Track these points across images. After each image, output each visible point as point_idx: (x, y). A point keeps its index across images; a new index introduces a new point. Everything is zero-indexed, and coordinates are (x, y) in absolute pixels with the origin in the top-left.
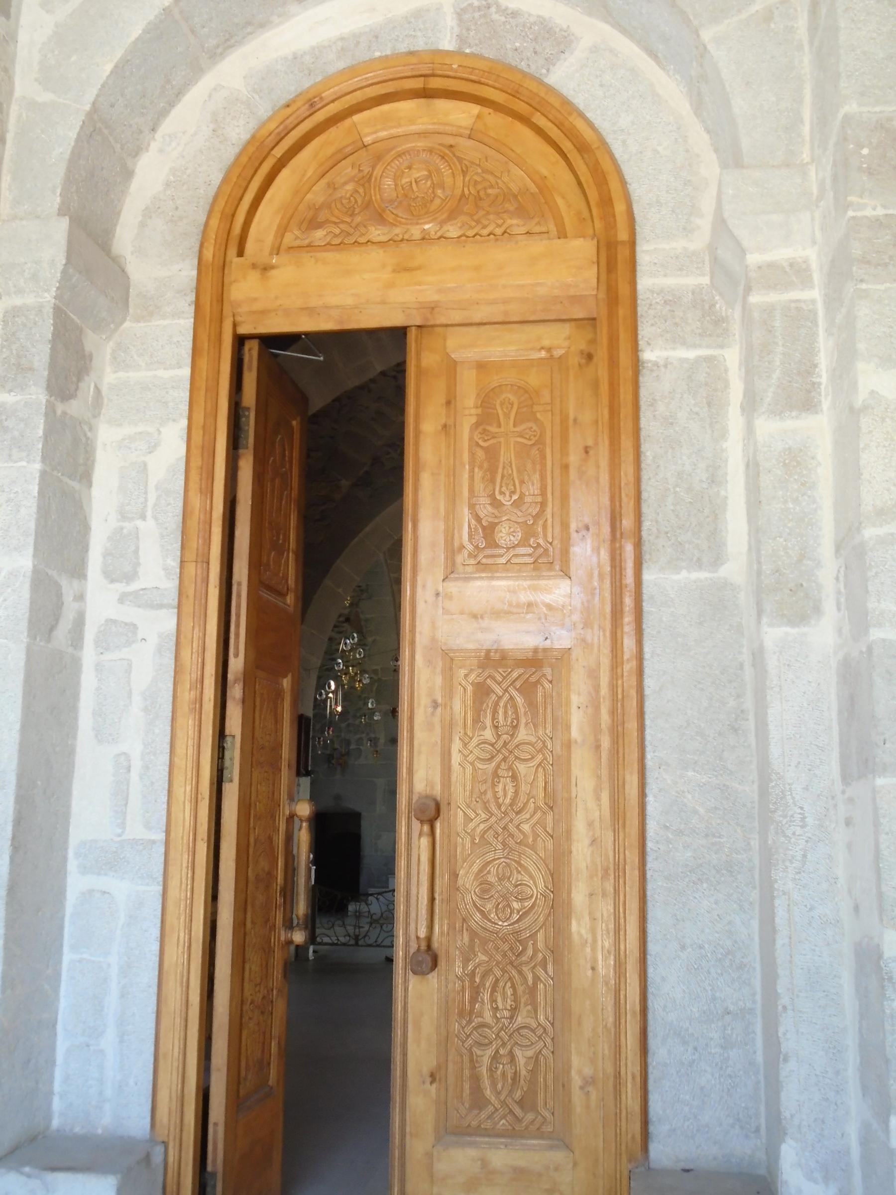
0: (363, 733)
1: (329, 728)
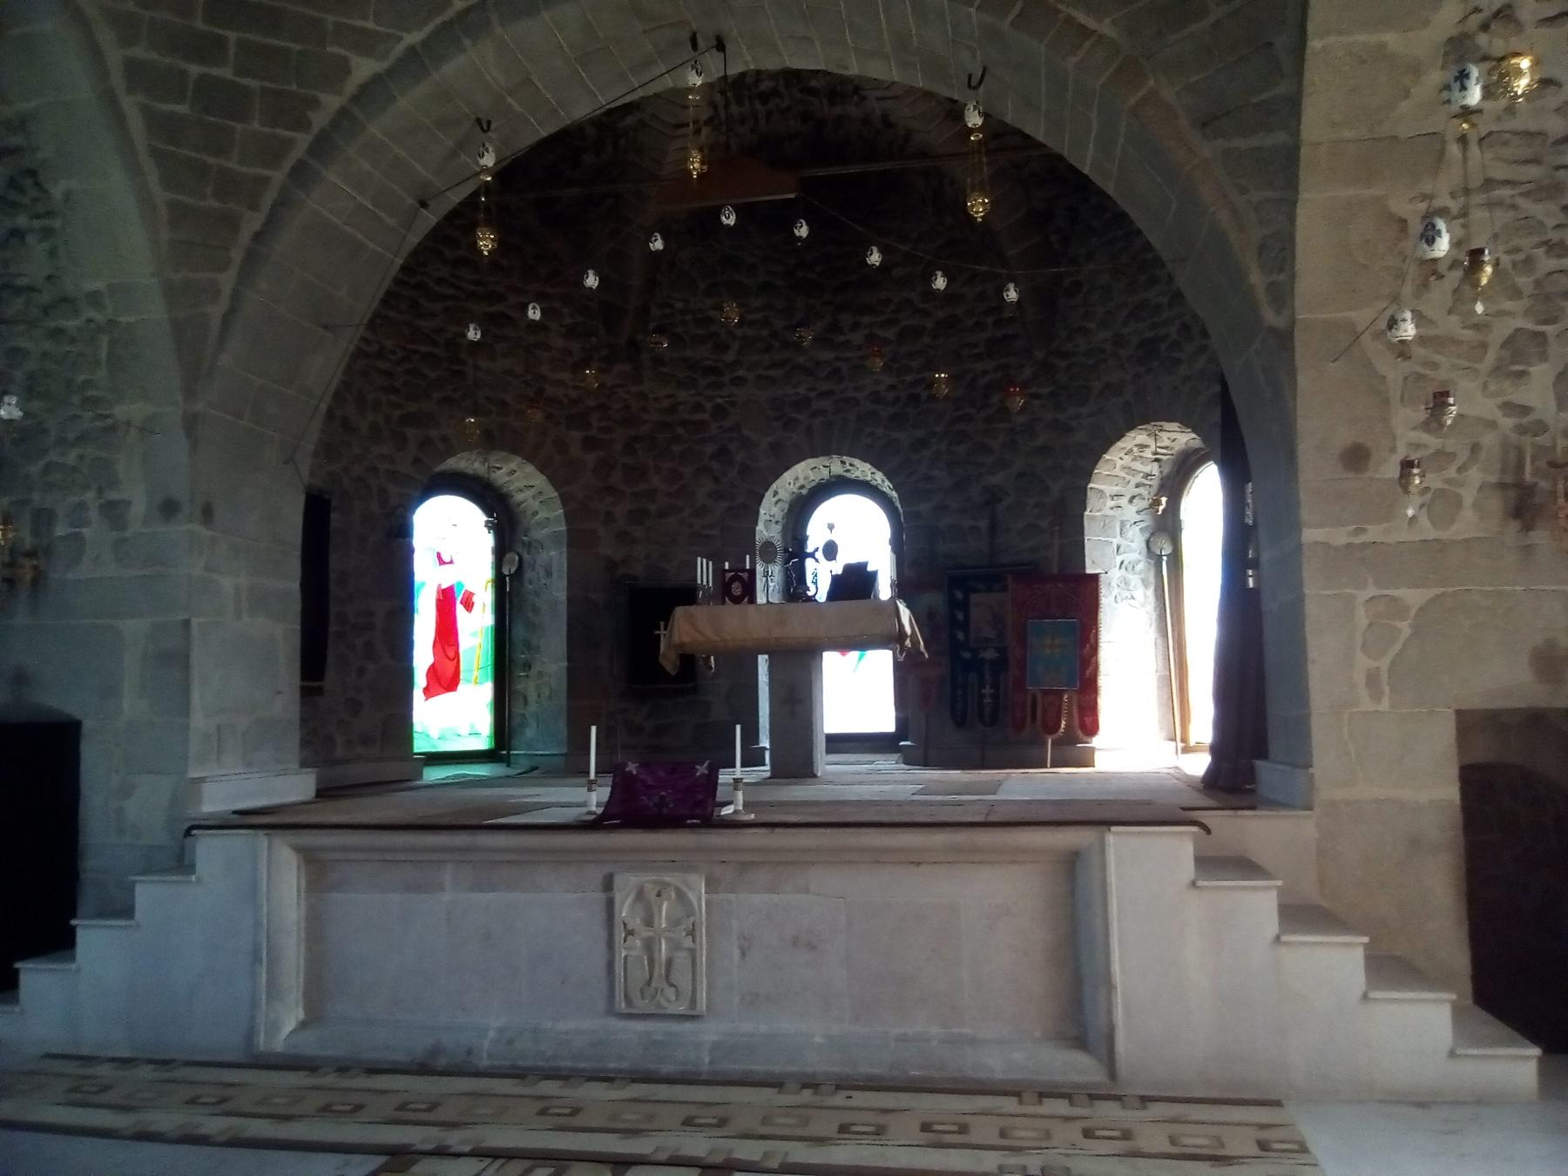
0: (86, 487)
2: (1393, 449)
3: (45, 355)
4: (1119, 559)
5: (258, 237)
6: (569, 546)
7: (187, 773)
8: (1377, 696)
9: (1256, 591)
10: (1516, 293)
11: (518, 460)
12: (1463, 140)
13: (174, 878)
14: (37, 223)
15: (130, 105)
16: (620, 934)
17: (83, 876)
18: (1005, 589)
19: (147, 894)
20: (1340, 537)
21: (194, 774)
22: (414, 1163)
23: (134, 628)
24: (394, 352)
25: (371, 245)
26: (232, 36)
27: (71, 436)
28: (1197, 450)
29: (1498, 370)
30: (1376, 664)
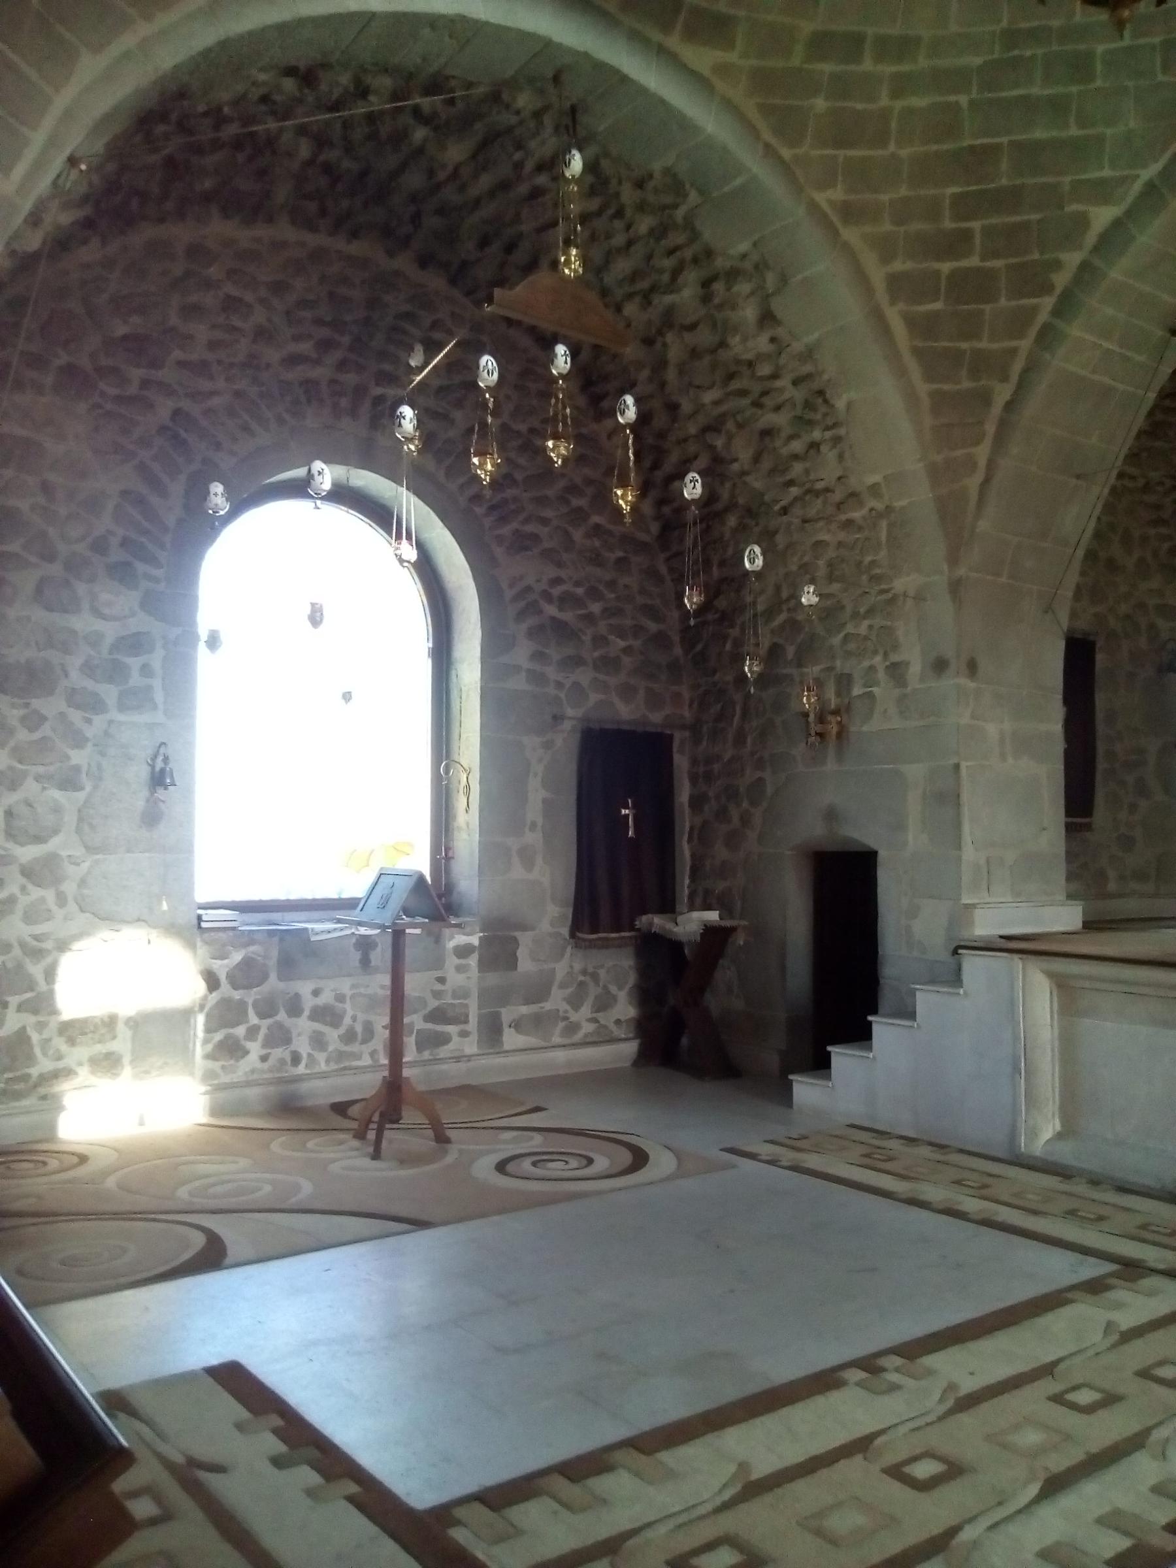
0: (875, 652)
3: (840, 544)
5: (1009, 406)
7: (960, 899)
13: (945, 990)
14: (828, 434)
15: (894, 317)
17: (882, 981)
19: (926, 1000)
21: (966, 900)
22: (1142, 1277)
23: (915, 772)
24: (1161, 483)
25: (1121, 387)
26: (976, 225)
27: (862, 610)
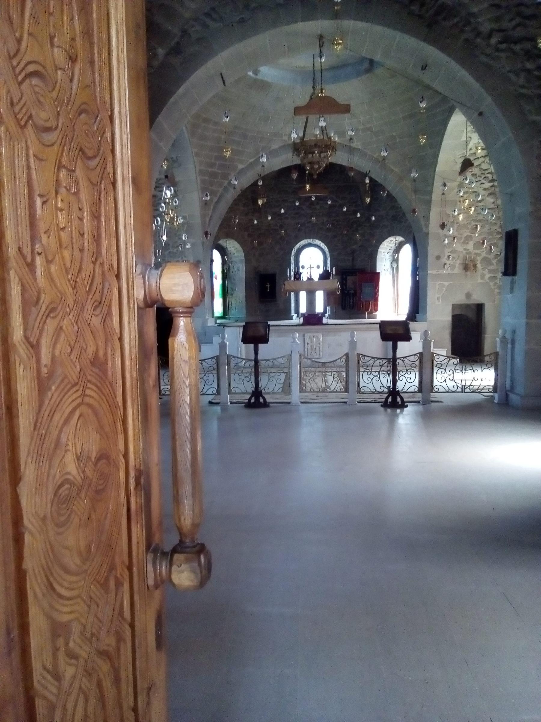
0: (179, 257)
1: (159, 251)
2: (445, 256)
4: (384, 268)
6: (245, 263)
8: (439, 301)
9: (418, 280)
10: (467, 228)
11: (233, 241)
12: (460, 201)
16: (306, 344)
18: (356, 275)
20: (434, 272)
26: (217, 162)
28: (404, 241)
29: (464, 243)
30: (438, 296)
